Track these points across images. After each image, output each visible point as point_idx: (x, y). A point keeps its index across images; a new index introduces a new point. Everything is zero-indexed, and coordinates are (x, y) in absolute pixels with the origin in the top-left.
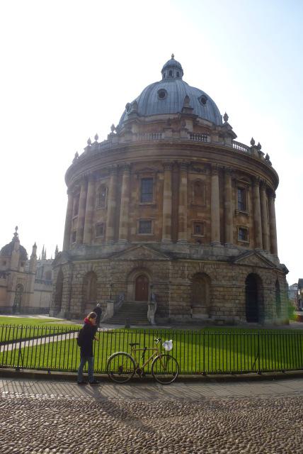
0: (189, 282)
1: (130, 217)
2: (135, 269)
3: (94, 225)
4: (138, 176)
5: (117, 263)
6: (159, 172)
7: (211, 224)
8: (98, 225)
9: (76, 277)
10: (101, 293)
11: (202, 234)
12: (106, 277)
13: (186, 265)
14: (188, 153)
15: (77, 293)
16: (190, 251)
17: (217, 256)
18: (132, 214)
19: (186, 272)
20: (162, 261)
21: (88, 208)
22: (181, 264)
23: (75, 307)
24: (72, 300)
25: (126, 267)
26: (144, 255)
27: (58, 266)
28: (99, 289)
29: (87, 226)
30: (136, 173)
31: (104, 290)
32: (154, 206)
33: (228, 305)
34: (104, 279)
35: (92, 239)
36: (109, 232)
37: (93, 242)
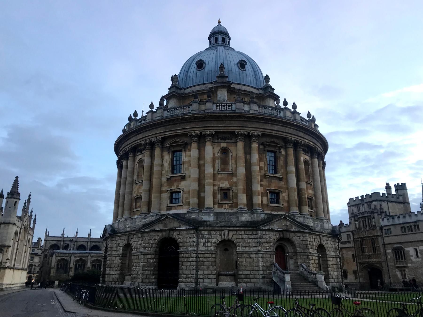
0: (317, 253)
1: (262, 186)
2: (279, 240)
3: (216, 188)
4: (265, 147)
5: (264, 233)
6: (282, 147)
7: (315, 200)
8: (222, 189)
9: (204, 245)
10: (244, 264)
11: (312, 209)
12: (250, 246)
13: (314, 237)
14: (301, 134)
15: (206, 264)
16: (314, 224)
17: (327, 230)
18: (262, 183)
19: (314, 243)
20: (301, 232)
21: (209, 170)
22: (311, 236)
23: (207, 281)
24: (200, 272)
25: (273, 237)
26: (287, 226)
27: (161, 231)
28: (241, 260)
29: (209, 189)
30: (263, 144)
31: (248, 260)
32: (280, 179)
33: (336, 273)
34: (247, 249)
35: (214, 203)
36: (243, 199)
37: (216, 206)
